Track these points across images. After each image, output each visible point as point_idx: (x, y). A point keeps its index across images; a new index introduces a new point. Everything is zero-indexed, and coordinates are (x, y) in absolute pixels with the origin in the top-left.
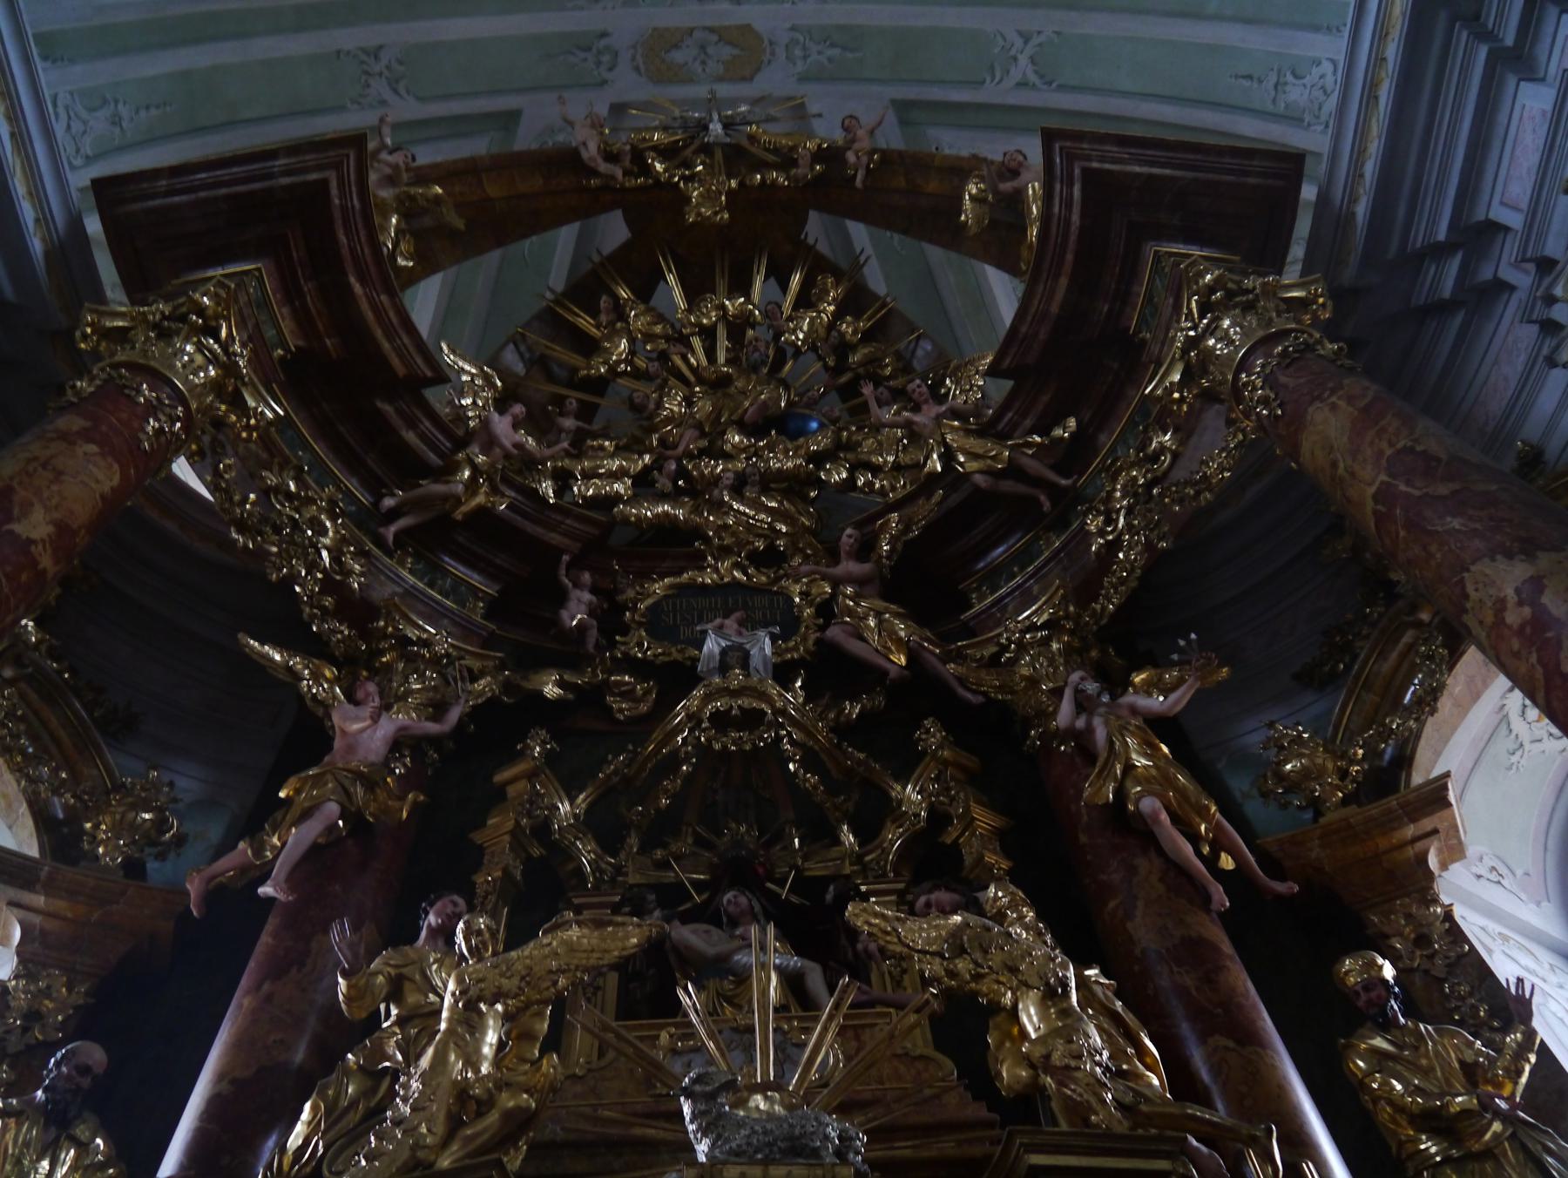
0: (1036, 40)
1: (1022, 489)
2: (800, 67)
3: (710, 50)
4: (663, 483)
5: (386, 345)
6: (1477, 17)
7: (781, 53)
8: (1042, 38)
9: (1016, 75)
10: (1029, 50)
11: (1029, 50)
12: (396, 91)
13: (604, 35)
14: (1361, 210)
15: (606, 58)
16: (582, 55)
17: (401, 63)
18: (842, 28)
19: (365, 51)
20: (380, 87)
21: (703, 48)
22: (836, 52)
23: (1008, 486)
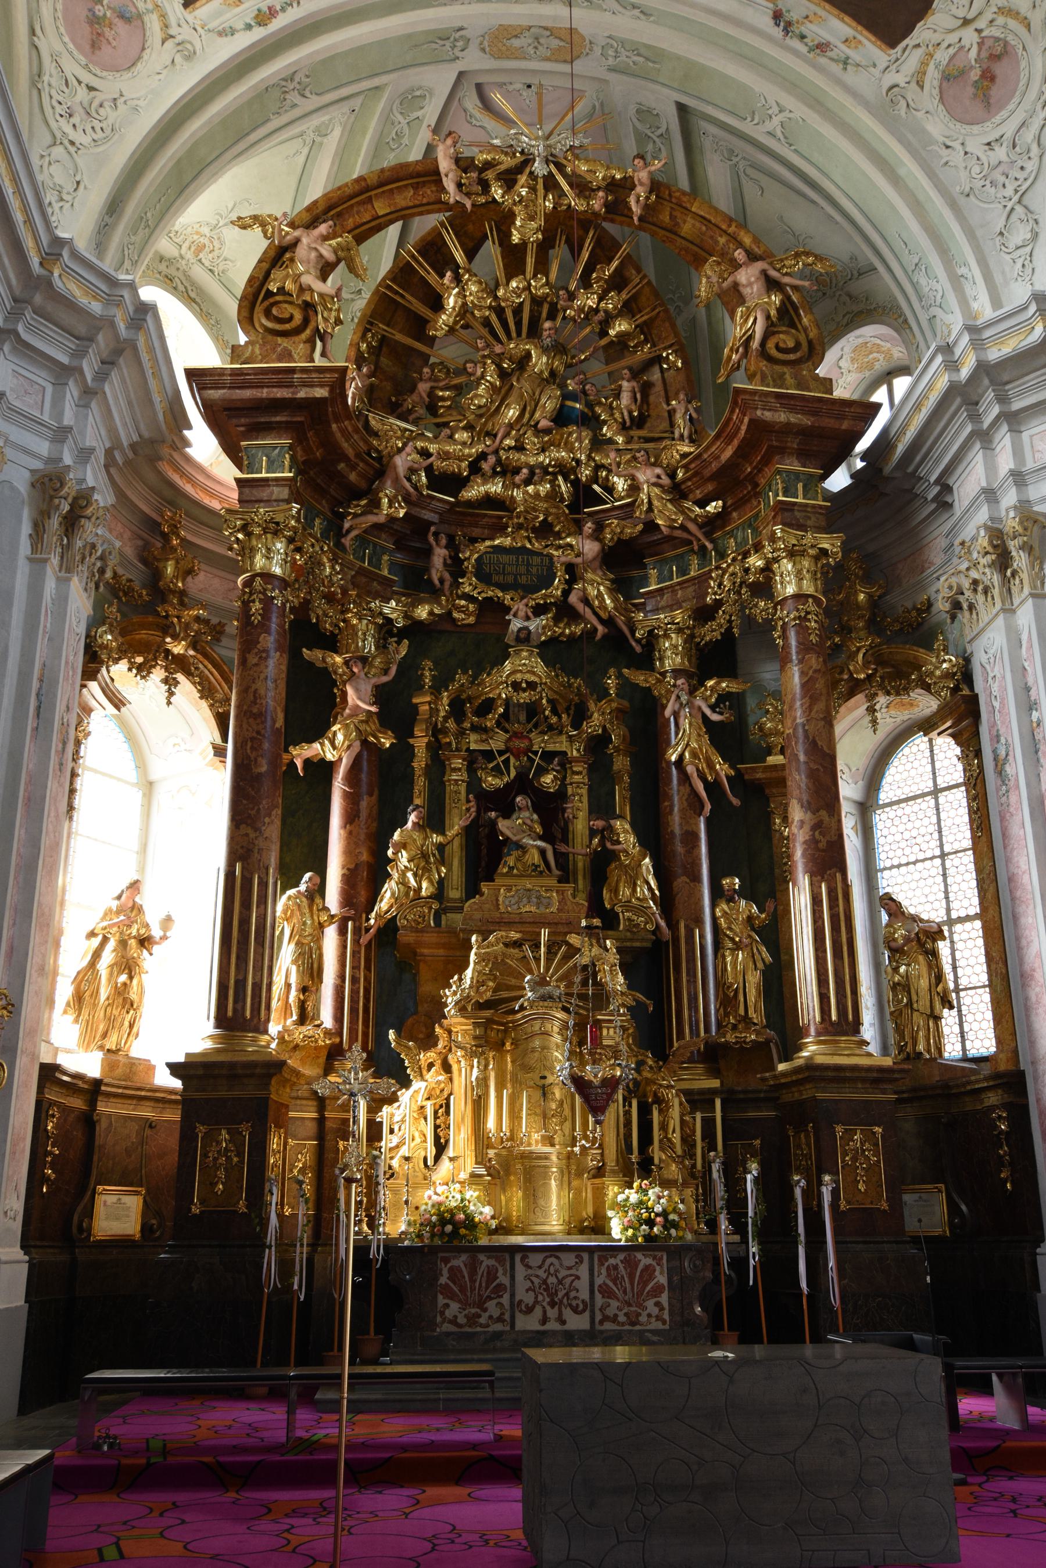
0: (786, 114)
1: (685, 535)
2: (611, 61)
3: (542, 41)
4: (486, 466)
5: (345, 445)
6: (977, 404)
7: (598, 51)
8: (791, 115)
9: (769, 126)
10: (781, 117)
11: (781, 117)
12: (304, 96)
13: (461, 29)
14: (900, 448)
15: (460, 44)
16: (442, 42)
17: (307, 76)
18: (648, 47)
19: (284, 80)
20: (294, 97)
21: (537, 39)
22: (641, 59)
23: (678, 533)
